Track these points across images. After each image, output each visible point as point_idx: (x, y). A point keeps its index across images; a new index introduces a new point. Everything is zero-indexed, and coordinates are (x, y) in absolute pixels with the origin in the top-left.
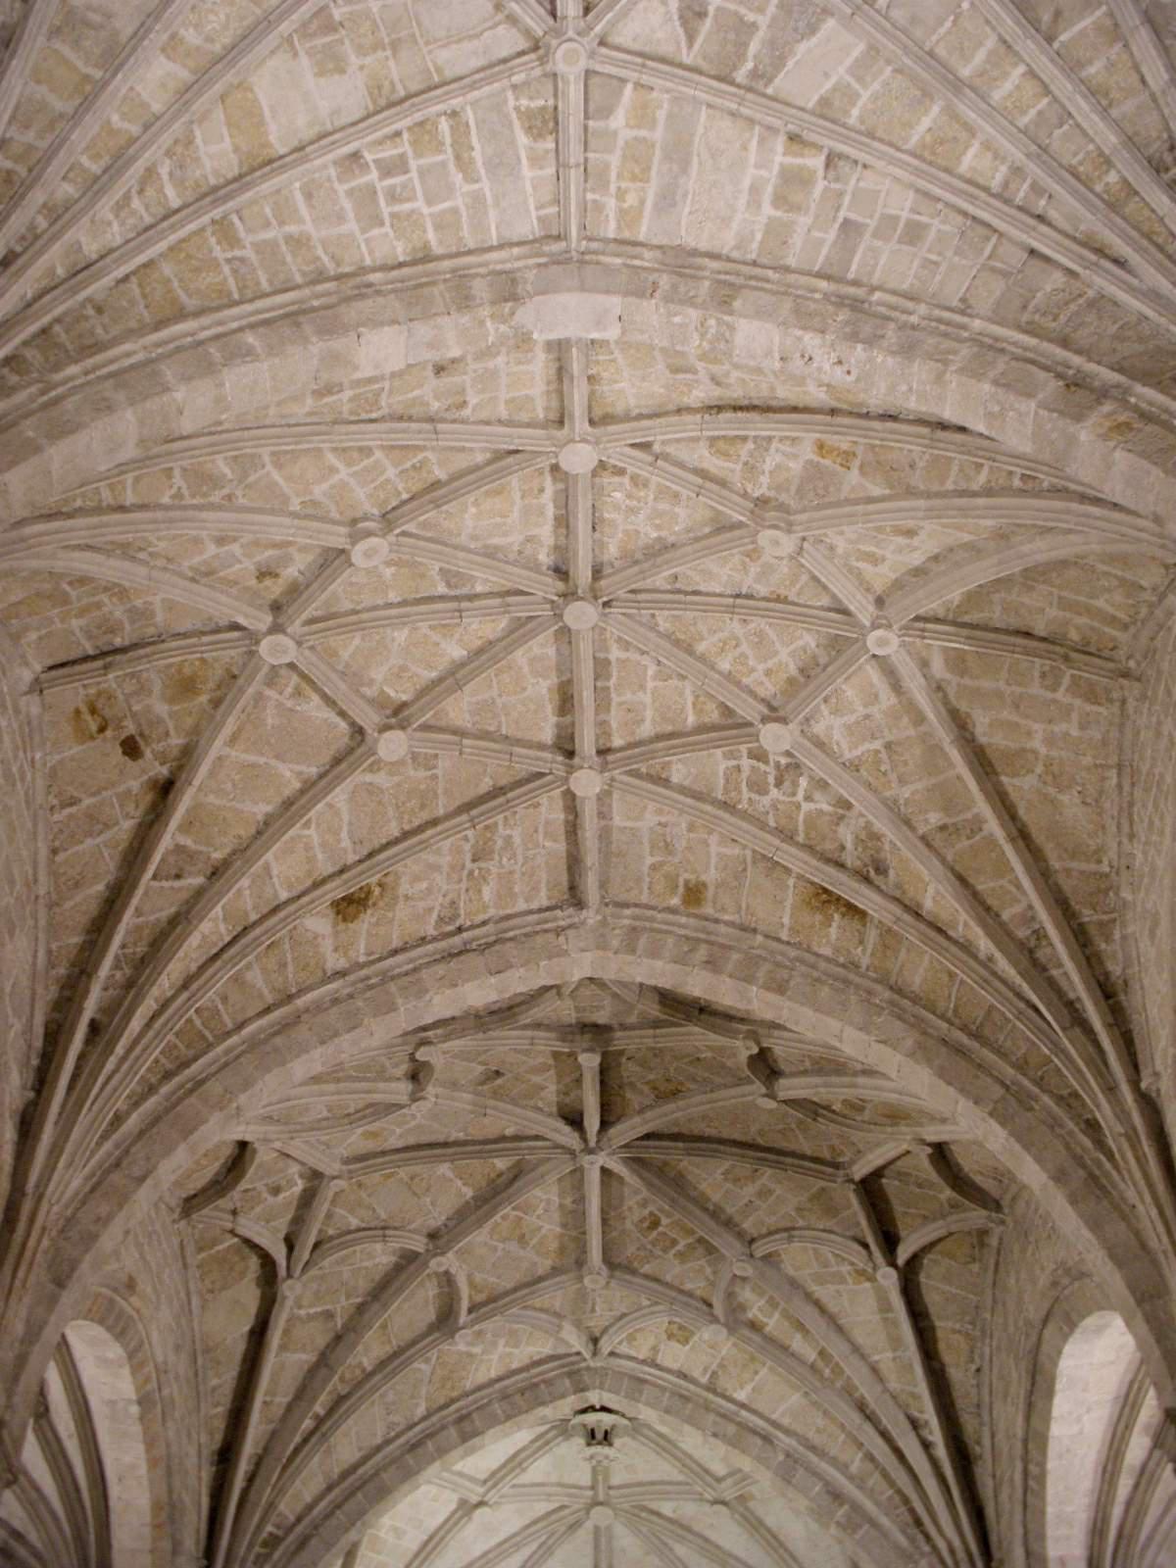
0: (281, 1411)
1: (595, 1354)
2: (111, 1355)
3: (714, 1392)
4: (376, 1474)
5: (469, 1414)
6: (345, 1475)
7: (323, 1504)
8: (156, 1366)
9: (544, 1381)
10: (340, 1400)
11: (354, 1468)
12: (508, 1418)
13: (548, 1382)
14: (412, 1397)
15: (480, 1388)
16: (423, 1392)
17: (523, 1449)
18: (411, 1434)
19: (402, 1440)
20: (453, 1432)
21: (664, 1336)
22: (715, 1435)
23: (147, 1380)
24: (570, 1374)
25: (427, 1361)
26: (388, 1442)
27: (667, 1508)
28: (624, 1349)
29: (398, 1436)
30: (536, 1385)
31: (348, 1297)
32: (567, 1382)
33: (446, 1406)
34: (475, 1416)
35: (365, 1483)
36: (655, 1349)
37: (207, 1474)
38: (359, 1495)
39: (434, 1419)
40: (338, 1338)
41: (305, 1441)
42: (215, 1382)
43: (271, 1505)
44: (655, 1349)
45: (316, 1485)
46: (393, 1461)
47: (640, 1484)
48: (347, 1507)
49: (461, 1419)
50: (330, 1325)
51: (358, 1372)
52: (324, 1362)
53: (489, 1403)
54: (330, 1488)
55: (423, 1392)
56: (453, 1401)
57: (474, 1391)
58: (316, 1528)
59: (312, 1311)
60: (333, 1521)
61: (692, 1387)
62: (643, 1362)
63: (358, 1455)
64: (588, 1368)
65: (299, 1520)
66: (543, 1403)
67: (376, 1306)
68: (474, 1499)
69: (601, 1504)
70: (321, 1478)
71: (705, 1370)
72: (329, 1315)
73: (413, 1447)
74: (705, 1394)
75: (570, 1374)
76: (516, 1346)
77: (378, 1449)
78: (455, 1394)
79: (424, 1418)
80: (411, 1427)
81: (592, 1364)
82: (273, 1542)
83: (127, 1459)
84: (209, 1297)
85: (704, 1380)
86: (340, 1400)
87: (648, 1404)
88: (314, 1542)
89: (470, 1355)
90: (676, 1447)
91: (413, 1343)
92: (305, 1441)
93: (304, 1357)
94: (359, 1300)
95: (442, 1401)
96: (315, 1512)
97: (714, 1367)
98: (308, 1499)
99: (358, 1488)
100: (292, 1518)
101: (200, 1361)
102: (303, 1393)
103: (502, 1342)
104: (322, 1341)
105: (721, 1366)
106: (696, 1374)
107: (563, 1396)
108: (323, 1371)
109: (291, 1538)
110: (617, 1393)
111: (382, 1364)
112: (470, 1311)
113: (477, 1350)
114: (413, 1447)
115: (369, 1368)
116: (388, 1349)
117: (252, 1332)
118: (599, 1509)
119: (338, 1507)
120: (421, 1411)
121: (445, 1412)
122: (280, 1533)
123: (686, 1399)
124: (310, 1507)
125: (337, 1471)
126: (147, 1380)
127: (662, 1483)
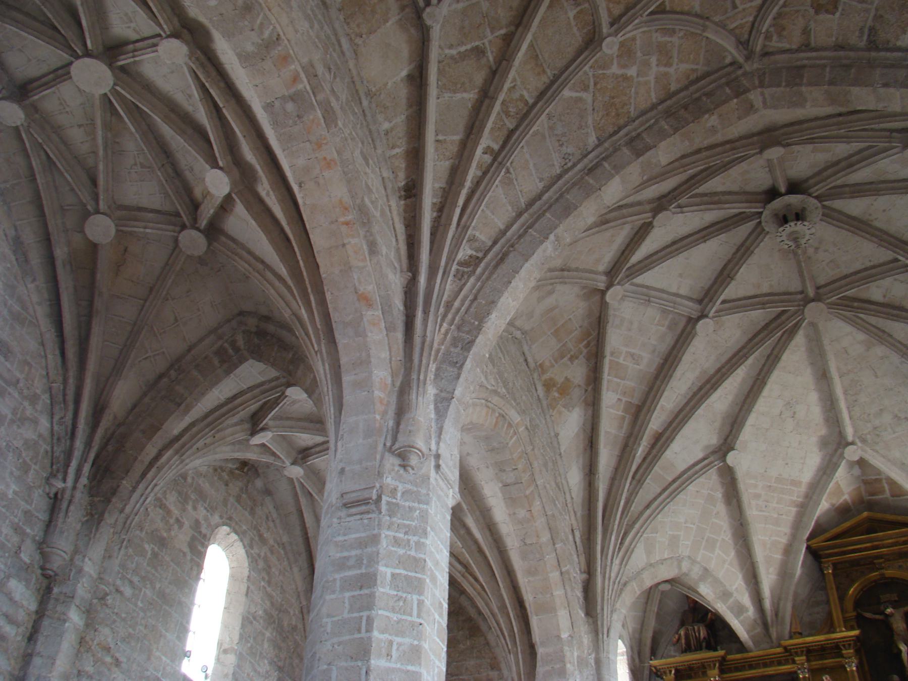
0: (454, 149)
1: (748, 58)
2: (250, 48)
3: (877, 49)
4: (561, 196)
5: (639, 134)
6: (530, 204)
7: (515, 227)
8: (303, 68)
9: (706, 95)
10: (511, 132)
11: (539, 197)
12: (676, 130)
13: (708, 95)
14: (580, 127)
15: (643, 113)
16: (590, 122)
17: (729, 261)
18: (586, 160)
19: (579, 167)
20: (626, 151)
21: (812, 11)
22: (886, 85)
23: (296, 79)
24: (728, 84)
25: (585, 89)
26: (567, 171)
27: (876, 291)
28: (775, 43)
29: (574, 165)
30: (698, 99)
31: (493, 30)
32: (728, 90)
33: (615, 133)
34: (644, 135)
35: (550, 206)
36: (806, 32)
37: (396, 206)
38: (548, 215)
39: (606, 145)
40: (494, 73)
41: (485, 173)
42: (386, 126)
43: (463, 228)
44: (806, 32)
45: (508, 212)
46: (574, 184)
47: (846, 277)
48: (537, 226)
49: (631, 142)
50: (483, 61)
51: (521, 105)
52: (486, 96)
53: (656, 122)
54: (520, 215)
55: (590, 122)
56: (620, 129)
57: (638, 118)
58: (512, 246)
59: (463, 49)
60: (527, 238)
61: (852, 54)
62: (798, 51)
63: (541, 185)
64: (745, 74)
65: (495, 243)
66: (707, 111)
67: (520, 29)
68: (695, 315)
69: (813, 300)
70: (510, 208)
71: (861, 30)
72: (479, 52)
73: (591, 171)
74: (866, 54)
75: (728, 84)
76: (668, 64)
77: (559, 177)
78: (621, 122)
79: (597, 146)
80: (586, 156)
81: (747, 67)
82: (473, 262)
83: (301, 162)
84: (359, 41)
85: (863, 44)
86: (511, 132)
87: (810, 84)
88: (511, 255)
89: (625, 78)
90: (870, 226)
91: (567, 67)
92: (485, 173)
93: (465, 95)
94: (503, 31)
95: (611, 130)
96: (509, 234)
97: (870, 23)
98: (502, 227)
99: (545, 211)
100: (490, 243)
101: (365, 103)
102: (473, 130)
103: (654, 60)
104: (479, 78)
105: (878, 17)
106: (854, 40)
107: (725, 102)
108: (487, 102)
109: (489, 257)
110: (779, 86)
111: (542, 94)
112: (612, 24)
113: (632, 72)
114: (591, 171)
115: (531, 101)
116: (545, 79)
117: (410, 78)
118: (813, 304)
119: (530, 227)
120: (592, 140)
121: (614, 138)
122: (480, 255)
123: (847, 67)
124: (503, 233)
125: (523, 201)
126: (296, 79)
127: (866, 269)
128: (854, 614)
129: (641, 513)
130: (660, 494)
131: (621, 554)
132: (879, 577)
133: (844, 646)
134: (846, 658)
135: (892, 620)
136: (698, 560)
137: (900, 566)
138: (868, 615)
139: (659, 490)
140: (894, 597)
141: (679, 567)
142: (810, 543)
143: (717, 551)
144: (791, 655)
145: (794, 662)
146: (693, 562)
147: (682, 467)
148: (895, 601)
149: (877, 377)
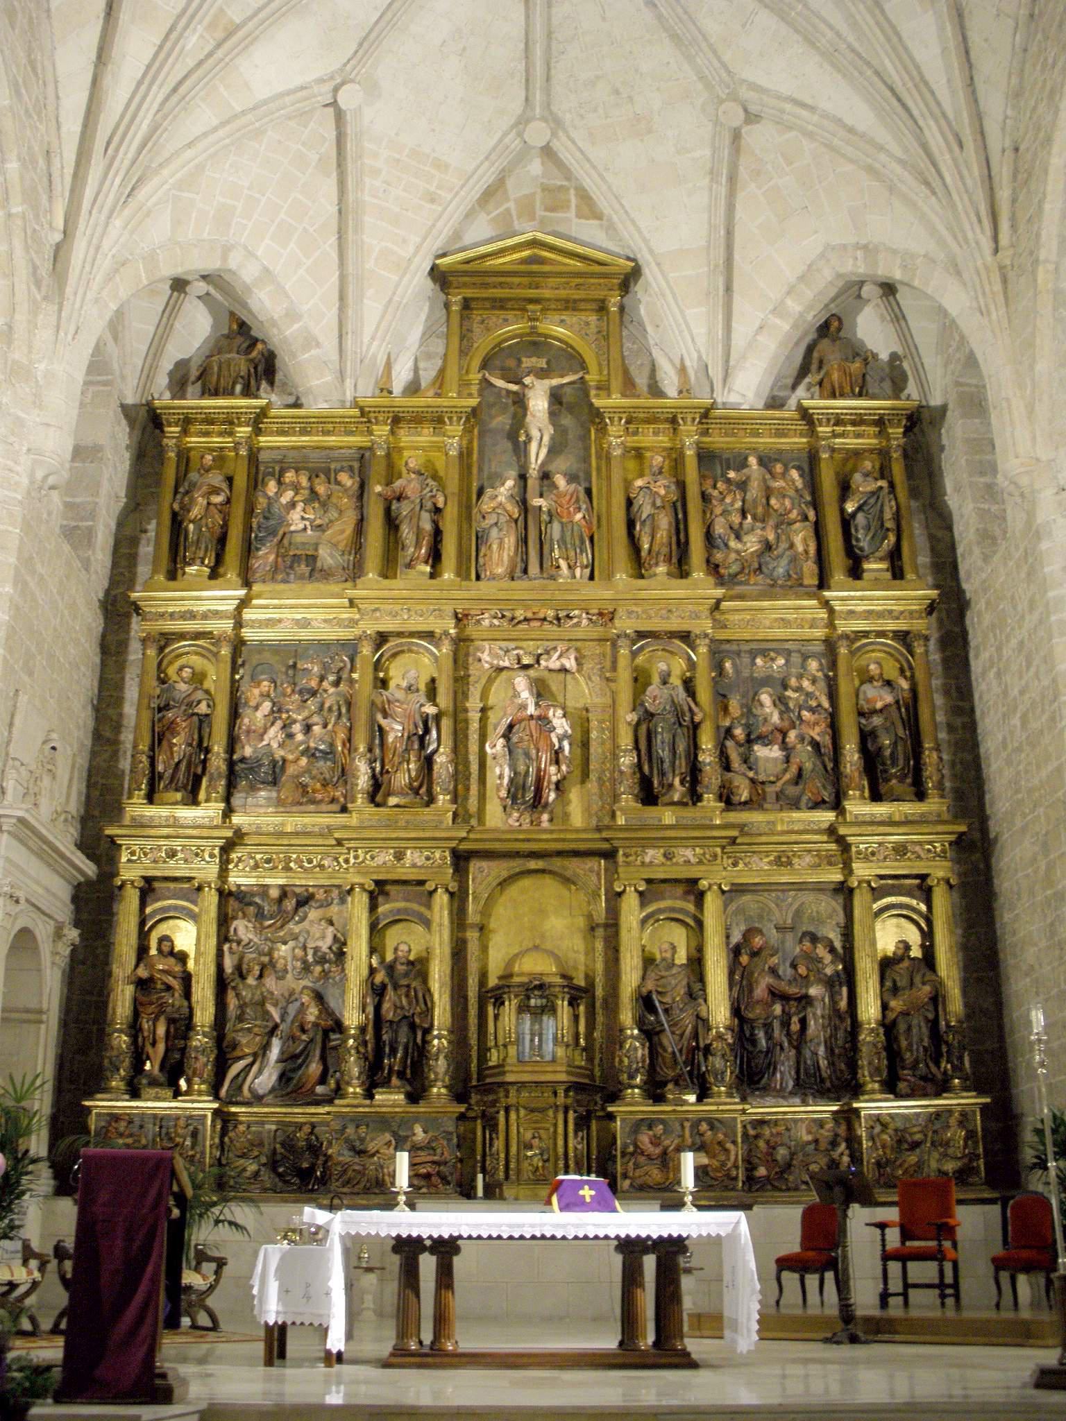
128: (480, 376)
129: (177, 153)
130: (215, 129)
131: (126, 212)
132: (528, 330)
133: (450, 419)
134: (449, 437)
135: (530, 394)
136: (259, 253)
137: (562, 321)
138: (500, 383)
139: (215, 122)
140: (542, 363)
141: (224, 258)
142: (438, 262)
143: (292, 245)
144: (369, 422)
145: (370, 433)
146: (251, 254)
147: (262, 93)
148: (542, 369)
149: (604, 19)
